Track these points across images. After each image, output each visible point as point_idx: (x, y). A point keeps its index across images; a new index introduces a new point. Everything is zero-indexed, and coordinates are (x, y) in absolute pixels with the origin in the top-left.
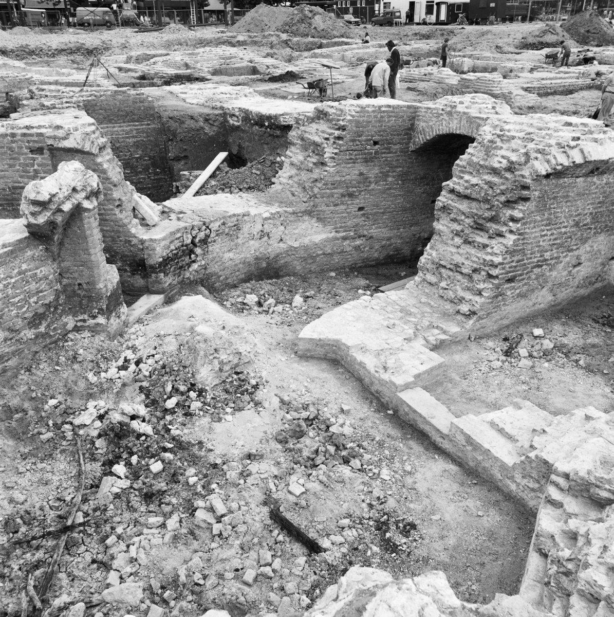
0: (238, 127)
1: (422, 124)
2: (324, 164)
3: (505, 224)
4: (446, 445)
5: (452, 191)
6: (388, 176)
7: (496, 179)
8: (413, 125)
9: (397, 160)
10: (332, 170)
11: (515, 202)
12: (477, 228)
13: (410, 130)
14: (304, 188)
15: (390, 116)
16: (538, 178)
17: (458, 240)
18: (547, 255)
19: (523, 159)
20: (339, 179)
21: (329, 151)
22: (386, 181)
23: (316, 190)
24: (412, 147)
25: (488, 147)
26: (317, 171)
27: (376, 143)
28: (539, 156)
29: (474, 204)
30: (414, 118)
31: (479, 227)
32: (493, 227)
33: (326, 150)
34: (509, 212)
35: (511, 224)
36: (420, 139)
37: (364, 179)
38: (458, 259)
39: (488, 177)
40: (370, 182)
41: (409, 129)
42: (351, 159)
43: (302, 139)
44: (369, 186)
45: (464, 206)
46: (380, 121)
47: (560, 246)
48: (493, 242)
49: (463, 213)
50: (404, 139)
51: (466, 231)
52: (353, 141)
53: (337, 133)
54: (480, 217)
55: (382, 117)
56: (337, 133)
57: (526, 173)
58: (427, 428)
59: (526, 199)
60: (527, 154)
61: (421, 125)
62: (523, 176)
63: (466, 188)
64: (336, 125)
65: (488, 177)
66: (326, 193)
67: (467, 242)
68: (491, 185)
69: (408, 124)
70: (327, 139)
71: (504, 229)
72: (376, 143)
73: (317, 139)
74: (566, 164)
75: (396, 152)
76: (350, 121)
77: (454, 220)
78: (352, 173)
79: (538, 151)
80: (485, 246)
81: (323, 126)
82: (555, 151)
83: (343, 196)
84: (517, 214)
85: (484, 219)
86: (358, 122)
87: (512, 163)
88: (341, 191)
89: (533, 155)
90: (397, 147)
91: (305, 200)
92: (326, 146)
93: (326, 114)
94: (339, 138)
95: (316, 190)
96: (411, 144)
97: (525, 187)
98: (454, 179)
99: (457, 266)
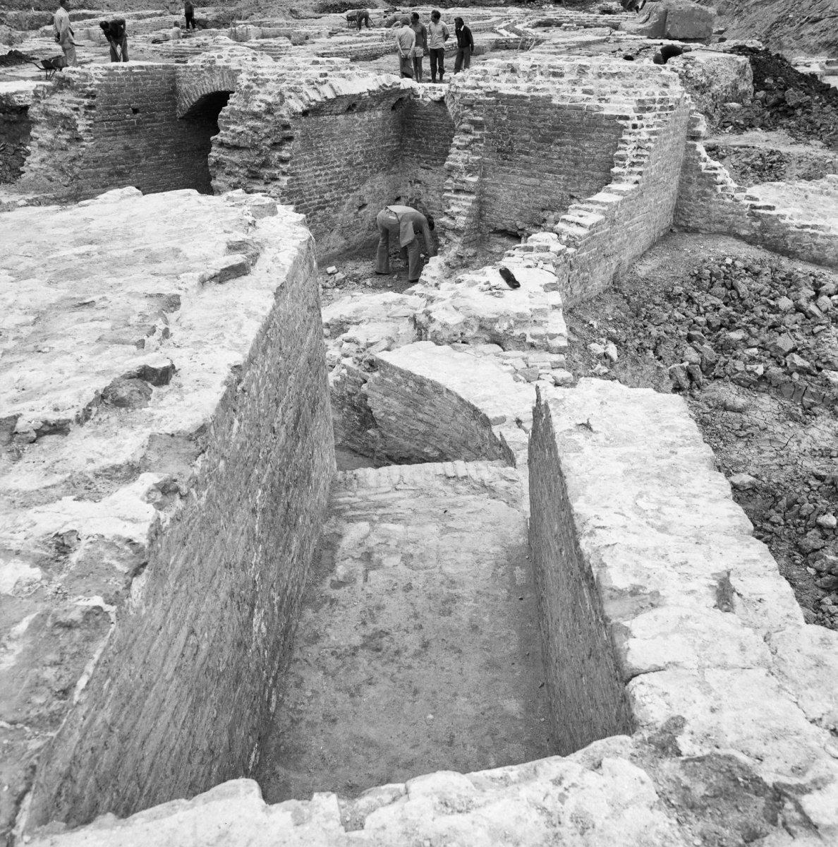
1: (185, 86)
2: (79, 139)
3: (277, 167)
5: (221, 144)
6: (159, 149)
7: (259, 124)
8: (174, 87)
9: (166, 130)
10: (90, 144)
11: (281, 143)
12: (253, 178)
13: (173, 93)
14: (62, 170)
15: (145, 79)
16: (295, 115)
18: (327, 196)
19: (278, 99)
20: (101, 155)
21: (82, 124)
22: (157, 154)
23: (77, 170)
24: (180, 114)
25: (246, 93)
26: (73, 148)
27: (135, 111)
28: (292, 94)
29: (245, 153)
30: (174, 80)
32: (266, 172)
33: (78, 122)
35: (281, 166)
36: (186, 103)
37: (130, 153)
39: (250, 123)
40: (139, 157)
41: (171, 93)
42: (110, 131)
44: (140, 162)
45: (235, 157)
46: (134, 85)
47: (339, 186)
48: (270, 187)
49: (236, 165)
50: (168, 104)
51: (243, 182)
52: (108, 109)
53: (86, 101)
54: (252, 164)
55: (135, 80)
56: (86, 101)
57: (284, 112)
59: (290, 139)
60: (280, 94)
61: (184, 87)
62: (282, 116)
63: (234, 138)
64: (83, 92)
65: (250, 123)
66: (89, 173)
69: (168, 87)
70: (76, 109)
71: (276, 172)
72: (135, 111)
73: (64, 111)
74: (319, 99)
75: (162, 121)
76: (98, 86)
77: (229, 174)
78: (116, 146)
79: (291, 90)
81: (68, 95)
82: (305, 88)
83: (111, 175)
84: (285, 154)
85: (257, 166)
86: (108, 87)
87: (269, 104)
88: (108, 169)
89: (287, 94)
90: (162, 114)
91: (66, 183)
92: (76, 117)
93: (68, 81)
94: (90, 107)
95: (77, 170)
96: (178, 111)
97: (286, 127)
98: (222, 132)
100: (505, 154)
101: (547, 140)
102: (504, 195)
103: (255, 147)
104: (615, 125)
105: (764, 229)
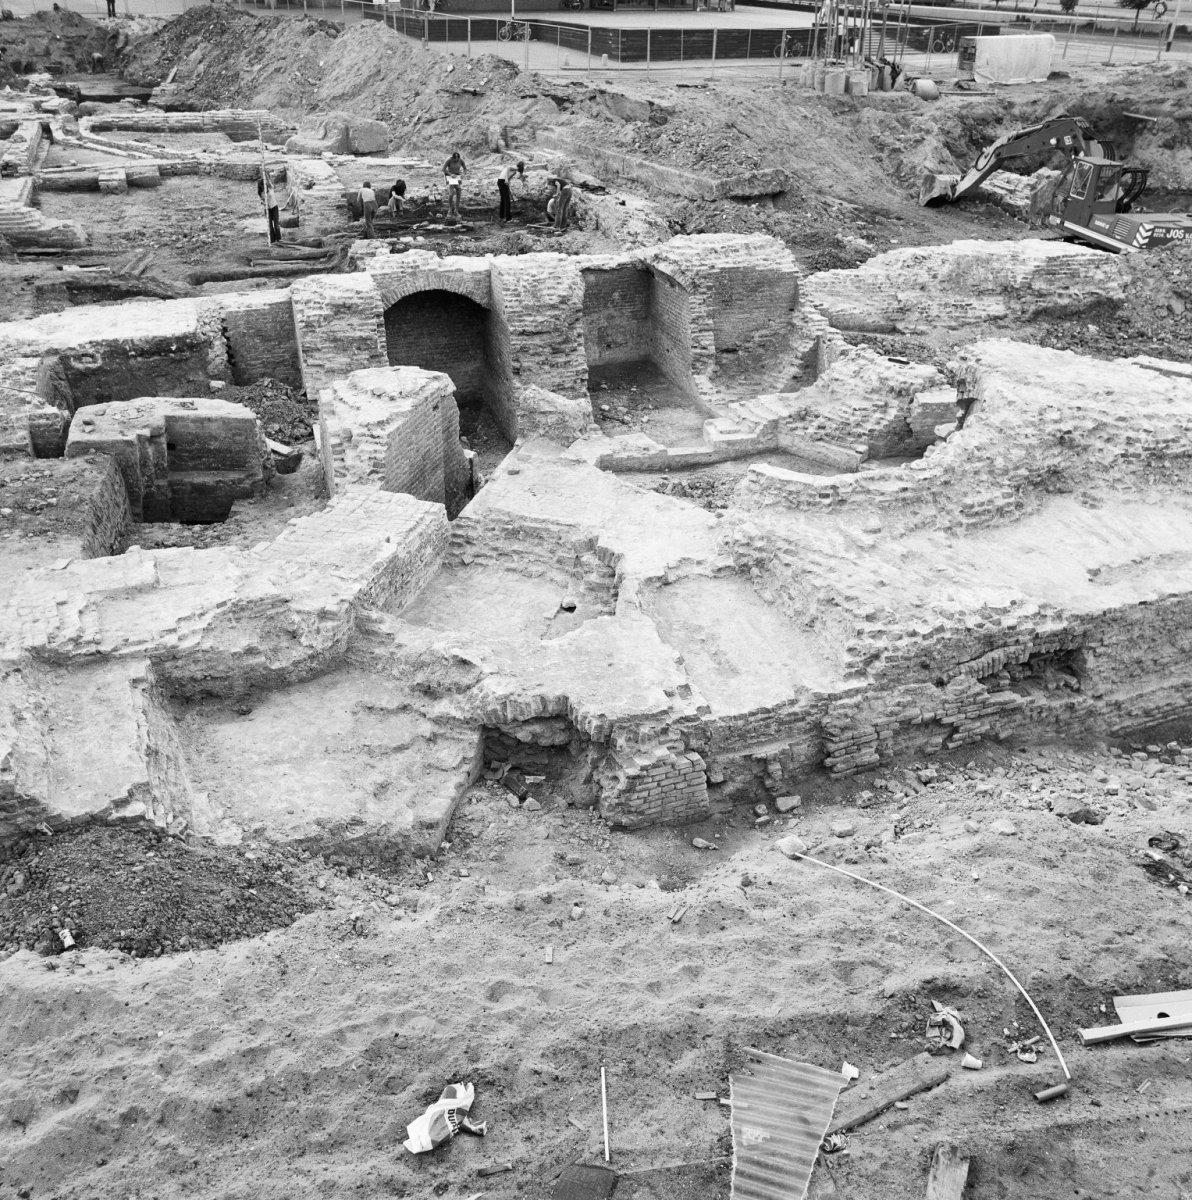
0: (99, 368)
4: (714, 458)
5: (523, 333)
17: (547, 367)
29: (545, 336)
31: (556, 351)
32: (567, 347)
34: (575, 333)
43: (335, 340)
45: (537, 340)
48: (573, 357)
58: (696, 459)
102: (727, 327)
103: (556, 330)
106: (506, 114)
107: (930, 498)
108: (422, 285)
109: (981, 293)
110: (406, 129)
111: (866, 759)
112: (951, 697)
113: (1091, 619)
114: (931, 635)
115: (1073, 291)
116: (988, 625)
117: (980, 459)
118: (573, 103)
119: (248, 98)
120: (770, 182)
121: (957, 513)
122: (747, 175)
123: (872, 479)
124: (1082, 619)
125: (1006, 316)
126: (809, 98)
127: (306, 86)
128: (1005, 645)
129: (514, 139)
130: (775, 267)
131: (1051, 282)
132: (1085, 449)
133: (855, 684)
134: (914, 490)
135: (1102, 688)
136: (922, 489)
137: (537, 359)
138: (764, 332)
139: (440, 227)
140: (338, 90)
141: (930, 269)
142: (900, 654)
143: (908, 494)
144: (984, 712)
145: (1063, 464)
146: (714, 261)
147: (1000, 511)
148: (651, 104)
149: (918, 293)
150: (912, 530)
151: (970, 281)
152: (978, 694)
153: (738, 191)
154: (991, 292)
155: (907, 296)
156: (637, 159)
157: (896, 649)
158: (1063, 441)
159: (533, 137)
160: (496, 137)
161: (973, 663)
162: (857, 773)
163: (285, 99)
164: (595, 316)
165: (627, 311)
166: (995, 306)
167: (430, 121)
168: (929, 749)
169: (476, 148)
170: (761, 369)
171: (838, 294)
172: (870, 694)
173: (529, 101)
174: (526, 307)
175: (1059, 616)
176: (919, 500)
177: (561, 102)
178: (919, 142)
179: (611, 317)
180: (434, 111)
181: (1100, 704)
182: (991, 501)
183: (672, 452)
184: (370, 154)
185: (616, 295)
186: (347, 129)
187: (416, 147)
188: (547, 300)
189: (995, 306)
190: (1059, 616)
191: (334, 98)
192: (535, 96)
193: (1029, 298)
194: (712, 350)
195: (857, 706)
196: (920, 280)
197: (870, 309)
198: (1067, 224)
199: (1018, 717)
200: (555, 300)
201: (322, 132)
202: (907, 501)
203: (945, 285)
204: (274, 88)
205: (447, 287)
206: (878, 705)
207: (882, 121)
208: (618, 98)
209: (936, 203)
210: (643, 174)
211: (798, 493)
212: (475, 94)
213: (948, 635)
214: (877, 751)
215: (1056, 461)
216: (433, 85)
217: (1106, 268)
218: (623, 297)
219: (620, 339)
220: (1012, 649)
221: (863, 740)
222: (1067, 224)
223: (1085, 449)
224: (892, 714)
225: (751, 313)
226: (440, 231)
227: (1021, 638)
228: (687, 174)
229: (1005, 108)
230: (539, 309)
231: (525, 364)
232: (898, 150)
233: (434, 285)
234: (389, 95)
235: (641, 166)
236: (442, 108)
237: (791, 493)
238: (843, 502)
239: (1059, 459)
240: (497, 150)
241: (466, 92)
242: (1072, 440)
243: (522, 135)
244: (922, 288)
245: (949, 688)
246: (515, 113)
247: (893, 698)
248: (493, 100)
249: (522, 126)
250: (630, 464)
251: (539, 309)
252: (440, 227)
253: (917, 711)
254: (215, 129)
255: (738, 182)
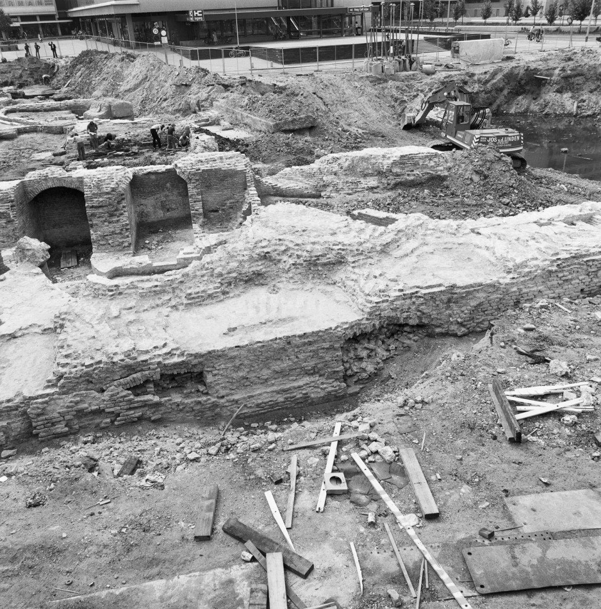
5: (92, 207)
17: (106, 223)
31: (111, 215)
32: (118, 213)
34: (121, 205)
38: (112, 229)
39: (108, 196)
45: (101, 210)
48: (121, 218)
59: (123, 199)
60: (117, 184)
65: (108, 196)
67: (110, 223)
68: (110, 199)
80: (118, 221)
97: (122, 195)
99: (113, 232)
100: (209, 187)
101: (222, 180)
102: (210, 199)
104: (243, 172)
105: (277, 191)
106: (199, 94)
107: (171, 290)
108: (50, 185)
109: (365, 176)
110: (154, 104)
111: (59, 430)
112: (107, 398)
113: (202, 356)
114: (91, 365)
115: (415, 172)
116: (127, 360)
117: (207, 269)
118: (232, 87)
119: (91, 93)
120: (305, 122)
121: (183, 298)
122: (290, 119)
123: (142, 281)
124: (196, 356)
125: (378, 187)
126: (362, 77)
127: (114, 87)
128: (142, 370)
129: (203, 106)
130: (233, 168)
131: (403, 169)
132: (279, 261)
133: (49, 391)
134: (161, 286)
135: (223, 392)
136: (166, 286)
137: (101, 219)
138: (231, 201)
139: (120, 153)
140: (128, 87)
141: (339, 164)
142: (72, 375)
143: (158, 289)
144: (132, 406)
145: (264, 270)
146: (200, 167)
147: (210, 296)
148: (275, 85)
149: (333, 176)
150: (153, 308)
151: (359, 170)
152: (125, 396)
153: (287, 127)
154: (372, 175)
155: (327, 178)
156: (245, 114)
157: (71, 373)
158: (266, 257)
159: (211, 105)
160: (194, 105)
161: (121, 380)
162: (55, 438)
163: (105, 92)
164: (158, 196)
165: (175, 192)
166: (373, 182)
167: (165, 100)
168: (103, 425)
169: (184, 112)
170: (229, 219)
171: (292, 179)
172: (56, 396)
173: (211, 87)
174: (94, 194)
175: (182, 354)
176: (164, 291)
177: (226, 87)
178: (415, 96)
179: (166, 196)
180: (168, 95)
181: (222, 401)
182: (204, 291)
183: (155, 264)
184: (120, 118)
185: (168, 185)
186: (110, 106)
187: (157, 113)
188: (105, 190)
189: (373, 182)
190: (182, 354)
191: (126, 91)
192: (213, 85)
193: (391, 177)
194: (201, 211)
195: (46, 402)
196: (334, 170)
197: (307, 186)
198: (448, 137)
199: (163, 408)
200: (109, 189)
201: (99, 108)
202: (156, 292)
203: (347, 172)
204: (102, 87)
205: (65, 185)
206: (61, 402)
207: (397, 87)
208: (258, 83)
209: (408, 128)
210: (247, 121)
211: (99, 289)
212: (186, 85)
213: (102, 365)
214: (66, 426)
215: (259, 268)
216: (170, 82)
217: (436, 160)
218: (172, 186)
219: (174, 206)
220: (147, 372)
221: (54, 420)
222: (448, 137)
223: (279, 261)
224: (68, 407)
225: (223, 192)
226: (121, 155)
227: (152, 367)
228: (263, 120)
229: (470, 77)
230: (100, 195)
231: (94, 222)
232: (405, 101)
233: (58, 185)
234: (150, 88)
235: (247, 117)
236: (171, 93)
237: (95, 289)
238: (120, 294)
239: (261, 267)
240: (195, 112)
241: (183, 85)
242: (270, 257)
243: (206, 104)
244: (335, 174)
245: (105, 393)
246: (203, 94)
247: (69, 399)
248: (194, 88)
249: (206, 100)
250: (132, 271)
251: (100, 195)
252: (120, 153)
253: (86, 405)
254: (66, 109)
255: (285, 123)
